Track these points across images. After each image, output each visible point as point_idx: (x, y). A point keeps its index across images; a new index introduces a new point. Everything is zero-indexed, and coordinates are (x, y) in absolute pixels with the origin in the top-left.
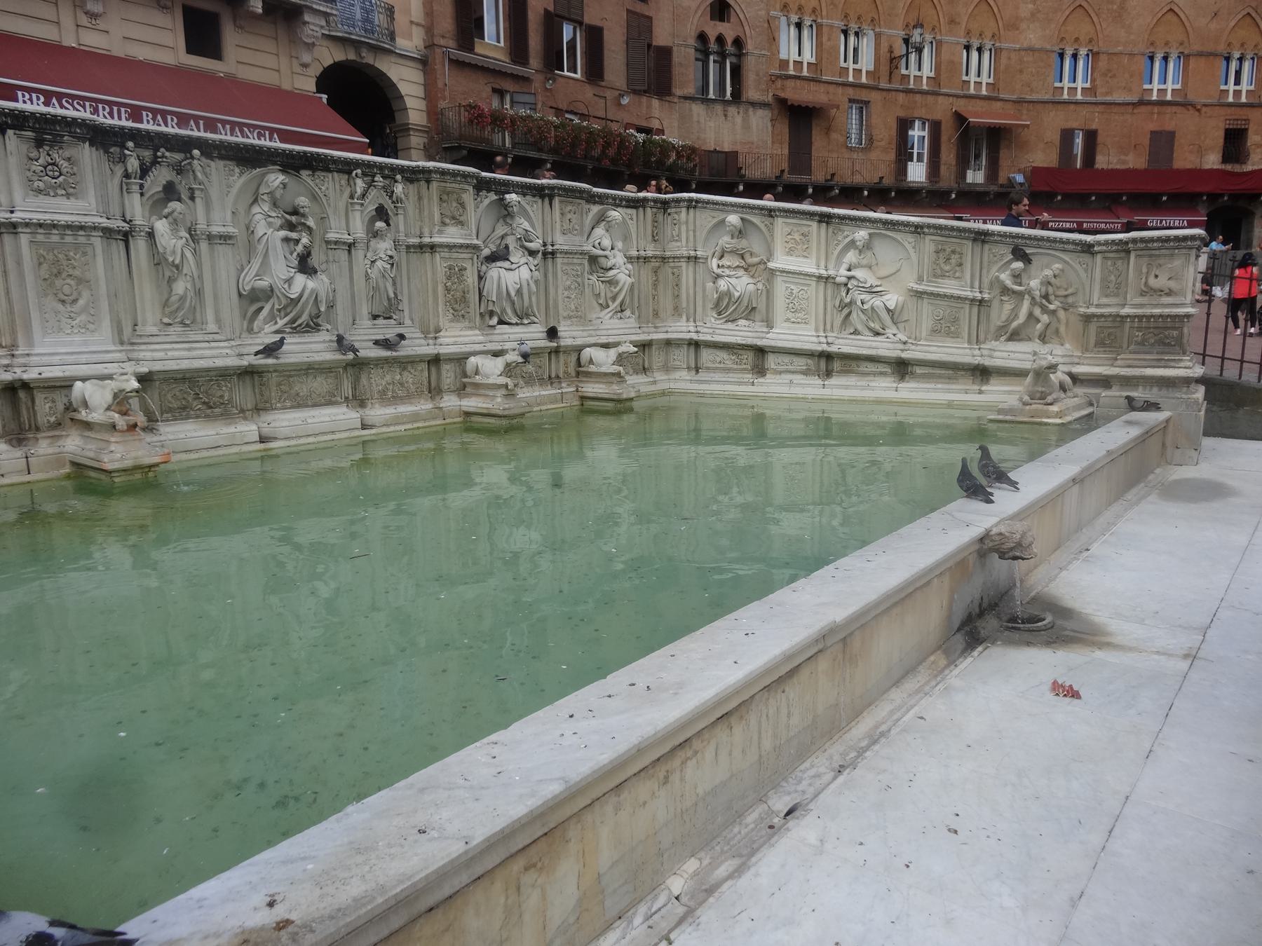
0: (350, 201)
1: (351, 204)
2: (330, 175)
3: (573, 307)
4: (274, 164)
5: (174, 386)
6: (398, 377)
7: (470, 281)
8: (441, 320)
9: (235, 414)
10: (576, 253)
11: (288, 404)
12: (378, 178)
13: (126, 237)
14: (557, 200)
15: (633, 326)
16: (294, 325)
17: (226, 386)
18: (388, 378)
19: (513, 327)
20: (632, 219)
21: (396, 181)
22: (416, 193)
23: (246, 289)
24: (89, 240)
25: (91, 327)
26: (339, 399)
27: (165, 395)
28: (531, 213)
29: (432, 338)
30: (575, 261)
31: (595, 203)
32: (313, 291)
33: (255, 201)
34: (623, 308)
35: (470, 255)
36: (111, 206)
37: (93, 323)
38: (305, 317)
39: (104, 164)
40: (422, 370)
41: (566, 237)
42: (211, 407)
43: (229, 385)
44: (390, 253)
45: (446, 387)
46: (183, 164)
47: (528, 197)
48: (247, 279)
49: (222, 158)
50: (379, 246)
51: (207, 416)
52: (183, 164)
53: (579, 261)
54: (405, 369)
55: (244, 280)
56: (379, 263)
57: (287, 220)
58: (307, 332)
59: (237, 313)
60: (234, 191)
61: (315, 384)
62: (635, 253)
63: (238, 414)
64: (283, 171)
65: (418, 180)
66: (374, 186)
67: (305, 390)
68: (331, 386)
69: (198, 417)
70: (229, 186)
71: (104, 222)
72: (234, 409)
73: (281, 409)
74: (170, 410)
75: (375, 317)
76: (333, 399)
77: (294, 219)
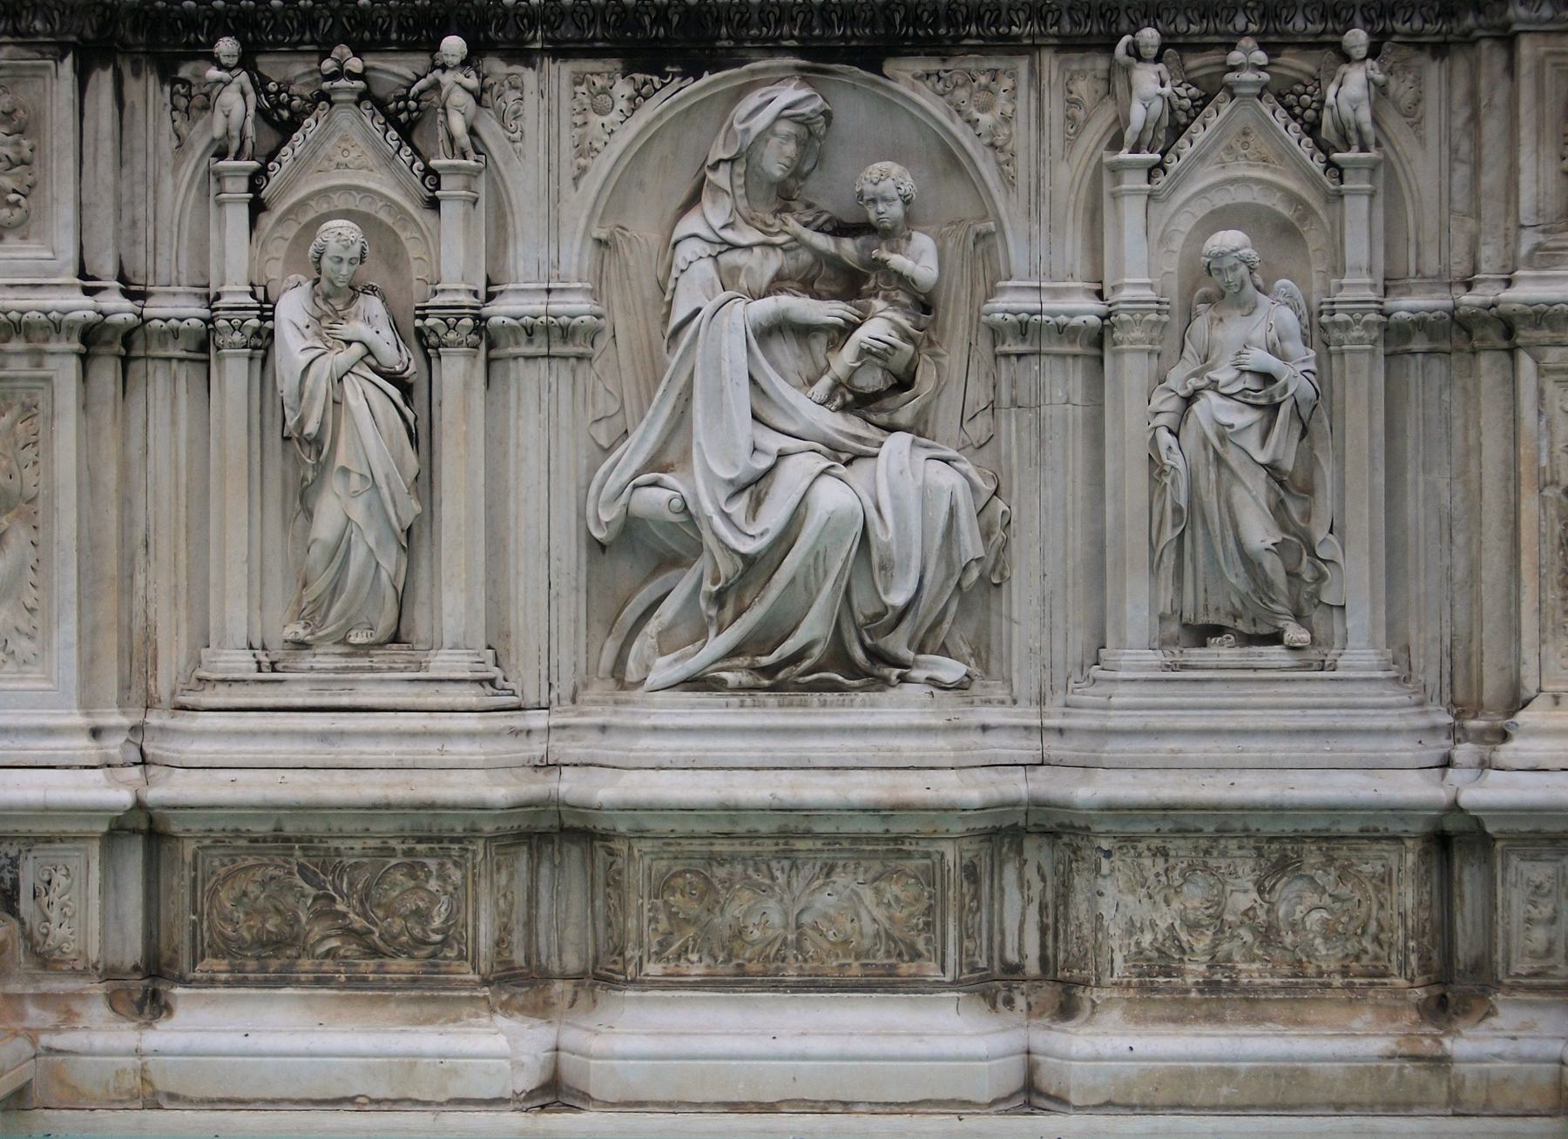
0: (1109, 158)
1: (1117, 169)
2: (1022, 65)
4: (774, 50)
5: (251, 861)
6: (1242, 899)
8: (1529, 654)
9: (464, 985)
11: (696, 968)
12: (1248, 53)
13: (204, 345)
16: (765, 660)
17: (443, 877)
18: (1194, 897)
21: (1347, 58)
22: (1460, 92)
23: (605, 518)
24: (39, 365)
25: (23, 646)
26: (931, 970)
27: (214, 892)
29: (1480, 736)
32: (833, 525)
33: (694, 200)
36: (163, 250)
37: (31, 637)
38: (813, 628)
39: (158, 118)
40: (1385, 879)
42: (374, 952)
43: (456, 875)
44: (1260, 358)
45: (1522, 966)
46: (414, 90)
48: (613, 484)
49: (561, 52)
50: (1218, 333)
51: (357, 982)
52: (414, 90)
54: (1283, 866)
55: (601, 487)
56: (1210, 408)
57: (819, 256)
58: (835, 687)
59: (571, 606)
60: (602, 165)
61: (825, 901)
63: (474, 986)
64: (805, 76)
65: (1469, 41)
66: (1231, 92)
67: (776, 918)
68: (899, 914)
69: (321, 981)
70: (585, 150)
71: (80, 307)
72: (467, 966)
73: (656, 984)
74: (226, 948)
75: (1203, 634)
76: (905, 968)
77: (849, 248)
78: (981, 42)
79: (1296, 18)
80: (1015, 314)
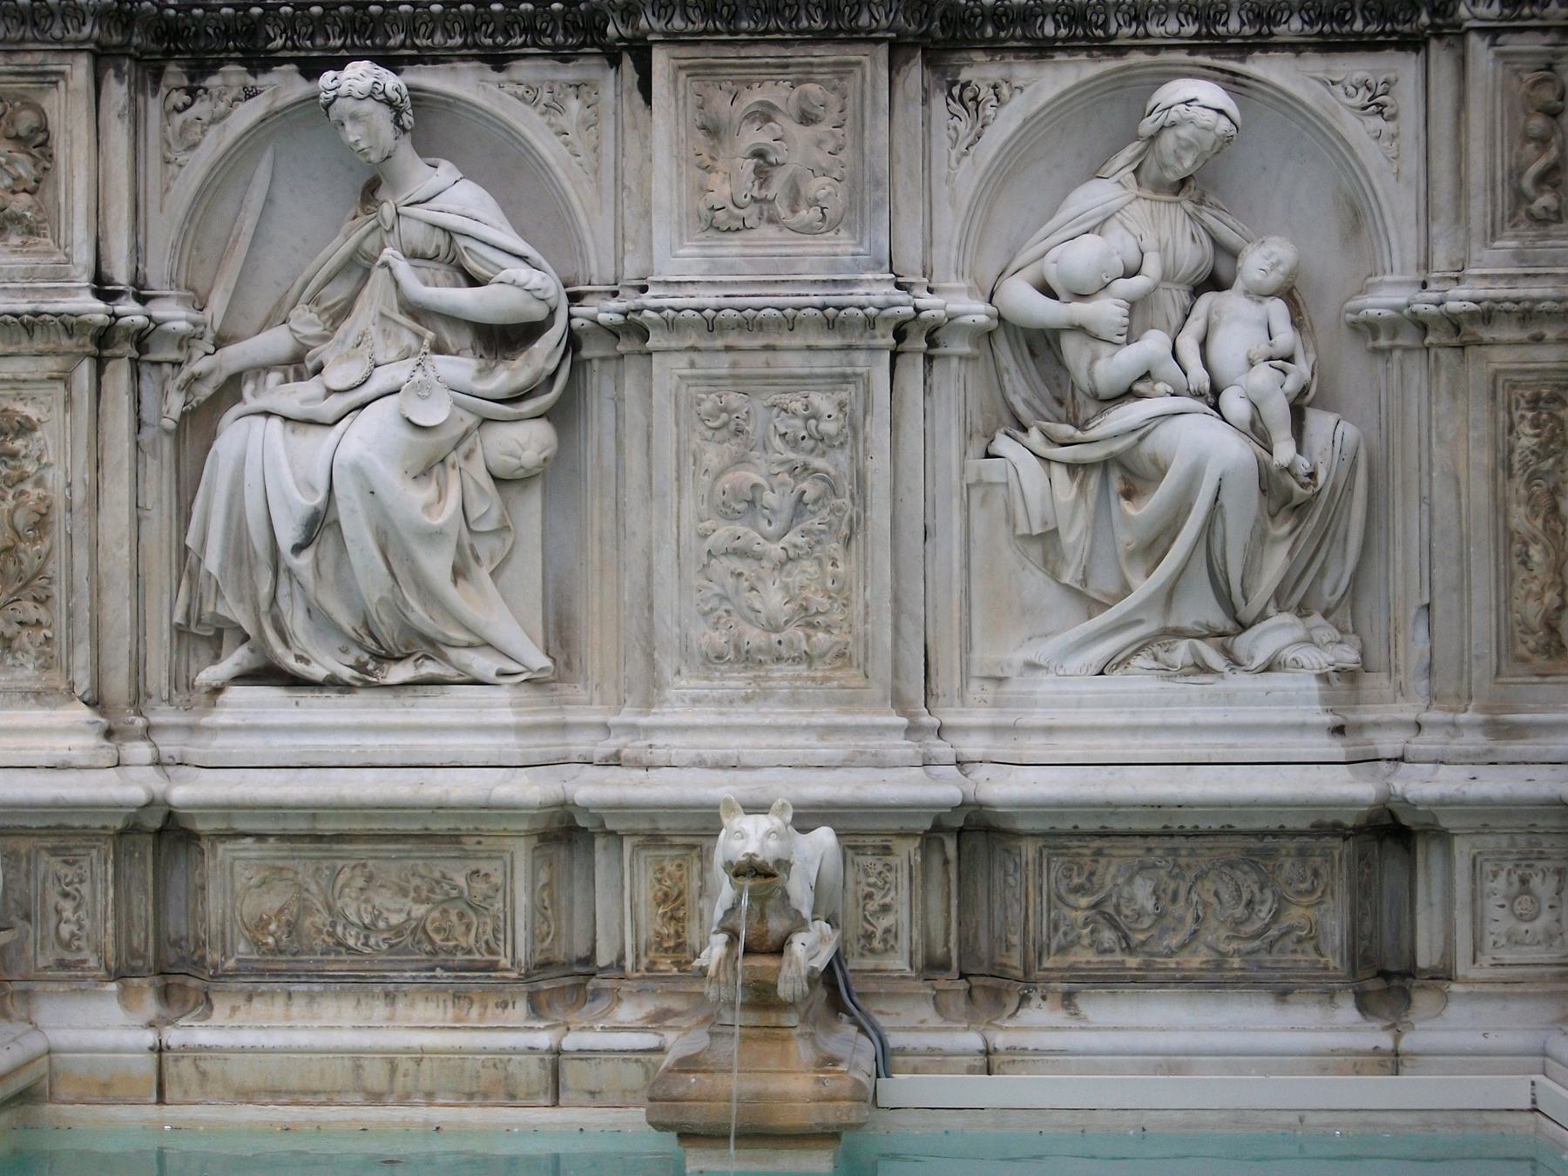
3: (773, 599)
7: (55, 478)
10: (792, 325)
14: (660, 60)
15: (1294, 716)
19: (308, 697)
20: (1378, 107)
28: (547, 146)
30: (794, 363)
31: (1041, 50)
34: (1247, 613)
35: (51, 365)
41: (732, 247)
47: (523, 70)
53: (821, 364)
62: (1384, 299)
78: (414, 52)
79: (1291, 20)
80: (781, 310)
